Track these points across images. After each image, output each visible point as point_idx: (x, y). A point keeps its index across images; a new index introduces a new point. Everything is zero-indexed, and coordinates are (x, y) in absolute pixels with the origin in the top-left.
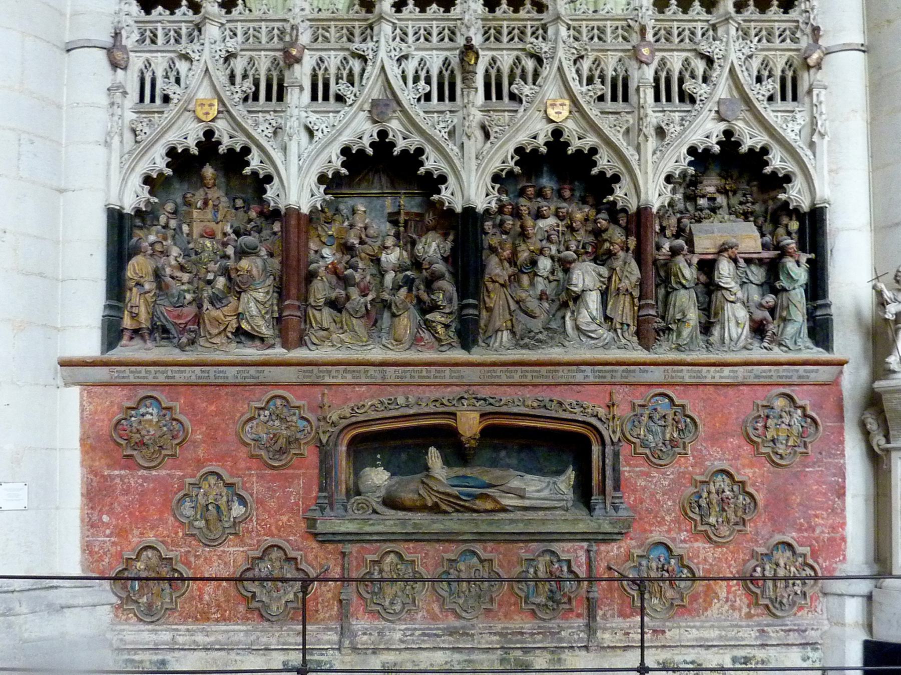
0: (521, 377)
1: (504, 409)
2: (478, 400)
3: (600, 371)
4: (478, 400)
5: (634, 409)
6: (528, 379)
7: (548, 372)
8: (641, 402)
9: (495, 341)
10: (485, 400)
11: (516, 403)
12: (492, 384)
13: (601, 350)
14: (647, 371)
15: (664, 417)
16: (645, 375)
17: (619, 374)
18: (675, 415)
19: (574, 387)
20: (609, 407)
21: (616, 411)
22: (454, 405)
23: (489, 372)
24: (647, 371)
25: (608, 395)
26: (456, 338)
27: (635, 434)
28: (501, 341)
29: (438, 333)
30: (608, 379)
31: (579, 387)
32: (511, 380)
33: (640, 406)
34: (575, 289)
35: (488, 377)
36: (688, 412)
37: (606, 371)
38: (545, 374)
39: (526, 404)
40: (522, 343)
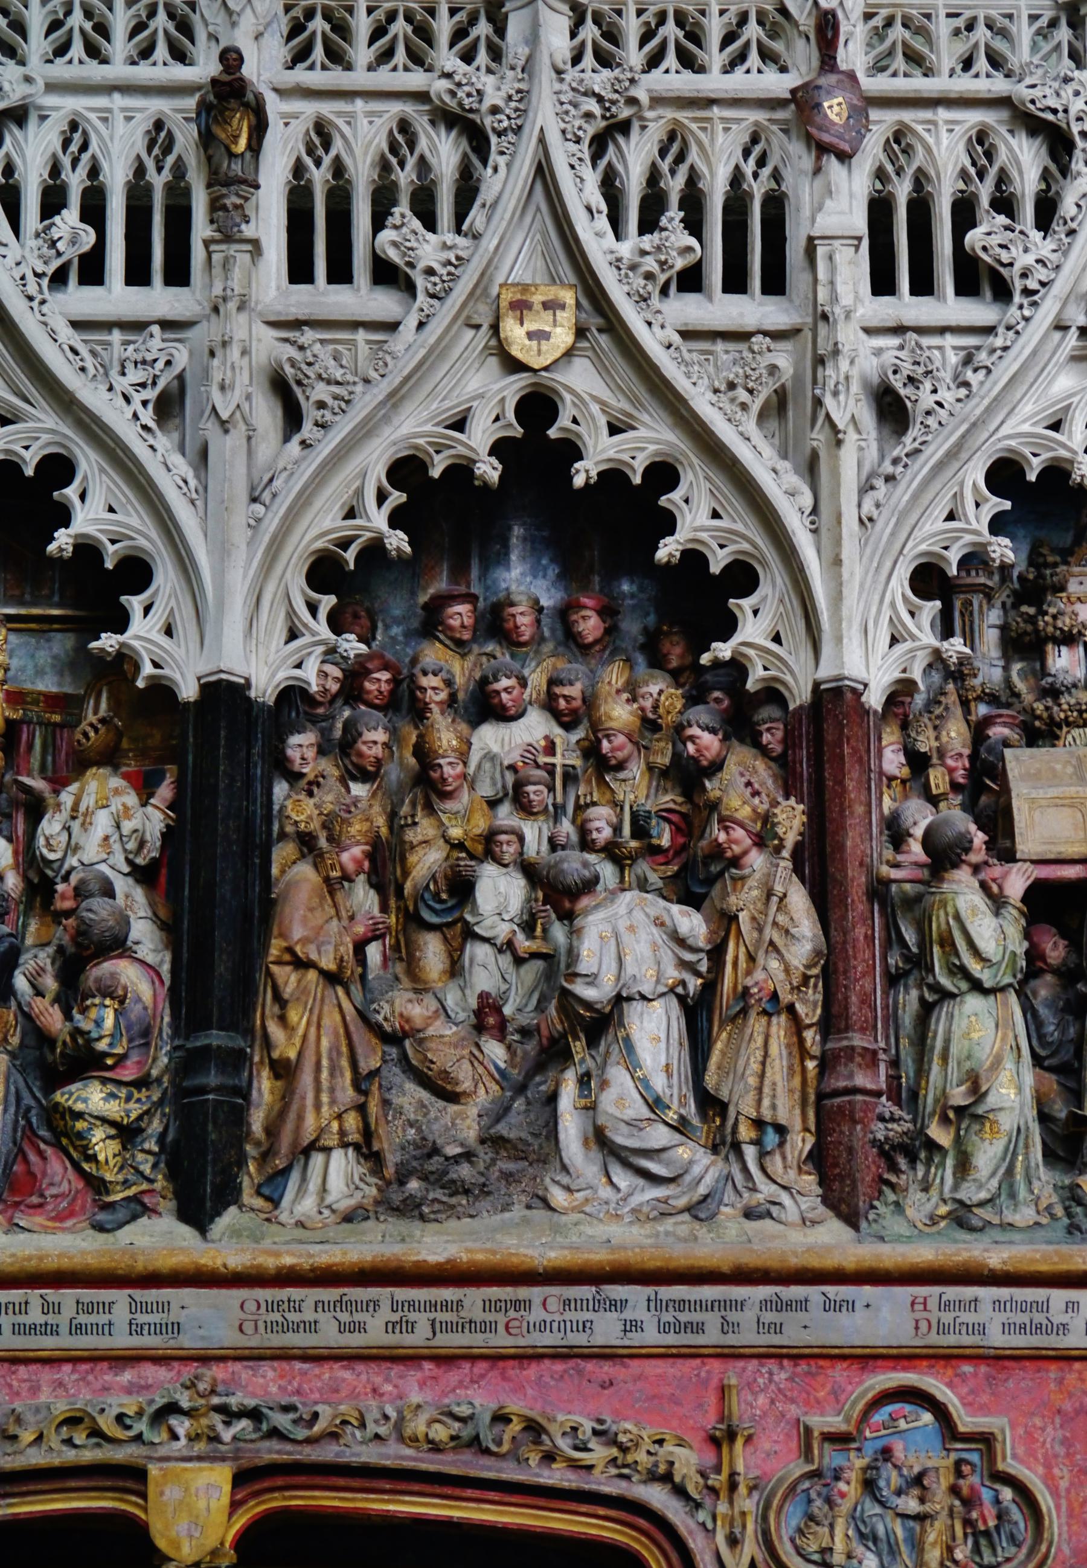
0: (391, 1327)
1: (328, 1453)
2: (229, 1415)
3: (681, 1305)
4: (229, 1415)
5: (807, 1453)
6: (418, 1337)
7: (489, 1305)
8: (835, 1422)
9: (301, 1190)
10: (255, 1414)
11: (372, 1428)
12: (283, 1355)
13: (683, 1225)
14: (851, 1306)
15: (918, 1480)
16: (844, 1318)
17: (747, 1318)
18: (959, 1474)
19: (589, 1366)
20: (715, 1442)
21: (742, 1459)
22: (139, 1438)
23: (271, 1307)
24: (851, 1306)
25: (712, 1399)
26: (160, 1183)
27: (812, 1547)
28: (324, 1190)
29: (93, 1158)
30: (712, 1336)
31: (607, 1369)
32: (355, 1340)
33: (830, 1438)
35: (270, 1327)
36: (1009, 1465)
37: (701, 1305)
38: (478, 1315)
39: (408, 1432)
40: (396, 1198)
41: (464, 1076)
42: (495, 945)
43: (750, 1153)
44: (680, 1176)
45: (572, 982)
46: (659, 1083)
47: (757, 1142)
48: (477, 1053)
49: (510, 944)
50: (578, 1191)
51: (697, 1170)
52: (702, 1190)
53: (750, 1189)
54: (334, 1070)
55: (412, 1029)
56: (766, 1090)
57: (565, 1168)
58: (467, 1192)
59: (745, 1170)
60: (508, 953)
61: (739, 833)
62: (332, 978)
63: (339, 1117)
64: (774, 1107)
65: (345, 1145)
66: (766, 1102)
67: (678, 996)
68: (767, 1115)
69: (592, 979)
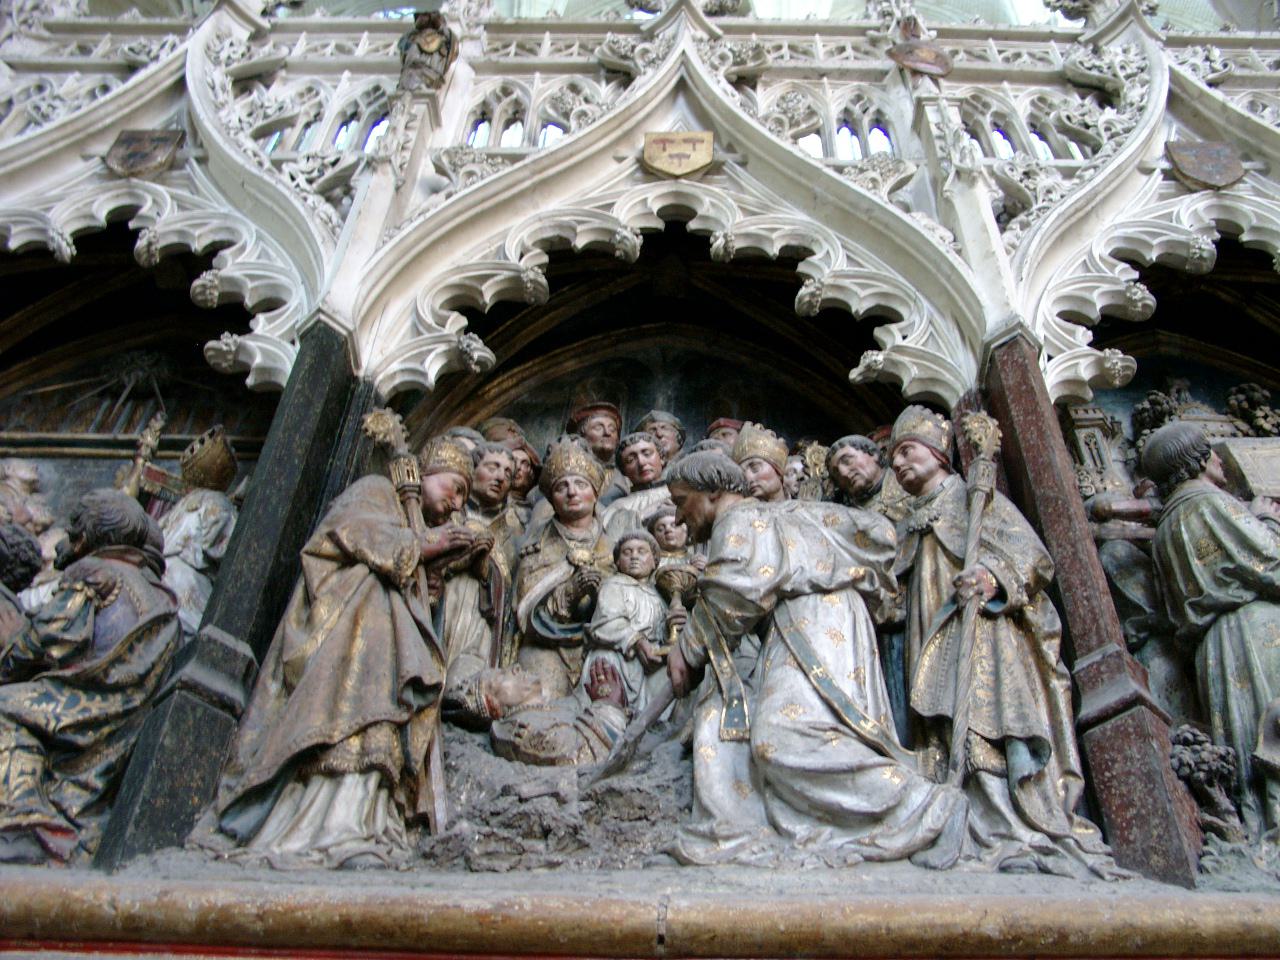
34: (740, 582)
41: (565, 740)
42: (620, 650)
43: (995, 786)
44: (889, 811)
45: (717, 573)
46: (848, 688)
47: (1004, 774)
48: (586, 717)
49: (637, 647)
50: (727, 838)
51: (917, 798)
52: (930, 821)
53: (1002, 837)
54: (367, 673)
55: (502, 704)
56: (1007, 699)
57: (707, 814)
58: (546, 833)
59: (990, 809)
60: (637, 662)
61: (921, 451)
62: (388, 580)
63: (362, 731)
64: (1022, 717)
65: (365, 770)
66: (1009, 714)
67: (865, 595)
68: (1016, 729)
69: (741, 565)
